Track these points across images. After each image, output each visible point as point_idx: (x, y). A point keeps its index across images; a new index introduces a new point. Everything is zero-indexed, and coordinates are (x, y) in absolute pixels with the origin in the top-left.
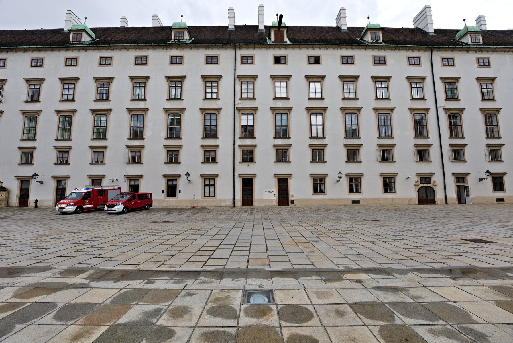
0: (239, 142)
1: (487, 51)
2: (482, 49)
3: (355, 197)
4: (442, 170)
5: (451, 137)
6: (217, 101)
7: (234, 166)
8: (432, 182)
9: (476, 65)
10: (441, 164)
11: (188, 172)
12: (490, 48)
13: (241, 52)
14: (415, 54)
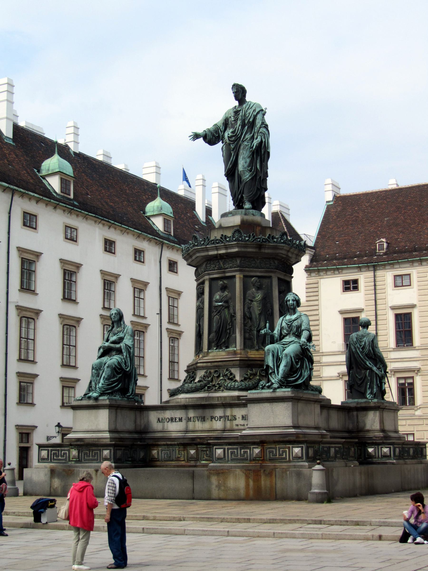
2: (72, 211)
5: (20, 360)
10: (3, 407)
12: (81, 212)
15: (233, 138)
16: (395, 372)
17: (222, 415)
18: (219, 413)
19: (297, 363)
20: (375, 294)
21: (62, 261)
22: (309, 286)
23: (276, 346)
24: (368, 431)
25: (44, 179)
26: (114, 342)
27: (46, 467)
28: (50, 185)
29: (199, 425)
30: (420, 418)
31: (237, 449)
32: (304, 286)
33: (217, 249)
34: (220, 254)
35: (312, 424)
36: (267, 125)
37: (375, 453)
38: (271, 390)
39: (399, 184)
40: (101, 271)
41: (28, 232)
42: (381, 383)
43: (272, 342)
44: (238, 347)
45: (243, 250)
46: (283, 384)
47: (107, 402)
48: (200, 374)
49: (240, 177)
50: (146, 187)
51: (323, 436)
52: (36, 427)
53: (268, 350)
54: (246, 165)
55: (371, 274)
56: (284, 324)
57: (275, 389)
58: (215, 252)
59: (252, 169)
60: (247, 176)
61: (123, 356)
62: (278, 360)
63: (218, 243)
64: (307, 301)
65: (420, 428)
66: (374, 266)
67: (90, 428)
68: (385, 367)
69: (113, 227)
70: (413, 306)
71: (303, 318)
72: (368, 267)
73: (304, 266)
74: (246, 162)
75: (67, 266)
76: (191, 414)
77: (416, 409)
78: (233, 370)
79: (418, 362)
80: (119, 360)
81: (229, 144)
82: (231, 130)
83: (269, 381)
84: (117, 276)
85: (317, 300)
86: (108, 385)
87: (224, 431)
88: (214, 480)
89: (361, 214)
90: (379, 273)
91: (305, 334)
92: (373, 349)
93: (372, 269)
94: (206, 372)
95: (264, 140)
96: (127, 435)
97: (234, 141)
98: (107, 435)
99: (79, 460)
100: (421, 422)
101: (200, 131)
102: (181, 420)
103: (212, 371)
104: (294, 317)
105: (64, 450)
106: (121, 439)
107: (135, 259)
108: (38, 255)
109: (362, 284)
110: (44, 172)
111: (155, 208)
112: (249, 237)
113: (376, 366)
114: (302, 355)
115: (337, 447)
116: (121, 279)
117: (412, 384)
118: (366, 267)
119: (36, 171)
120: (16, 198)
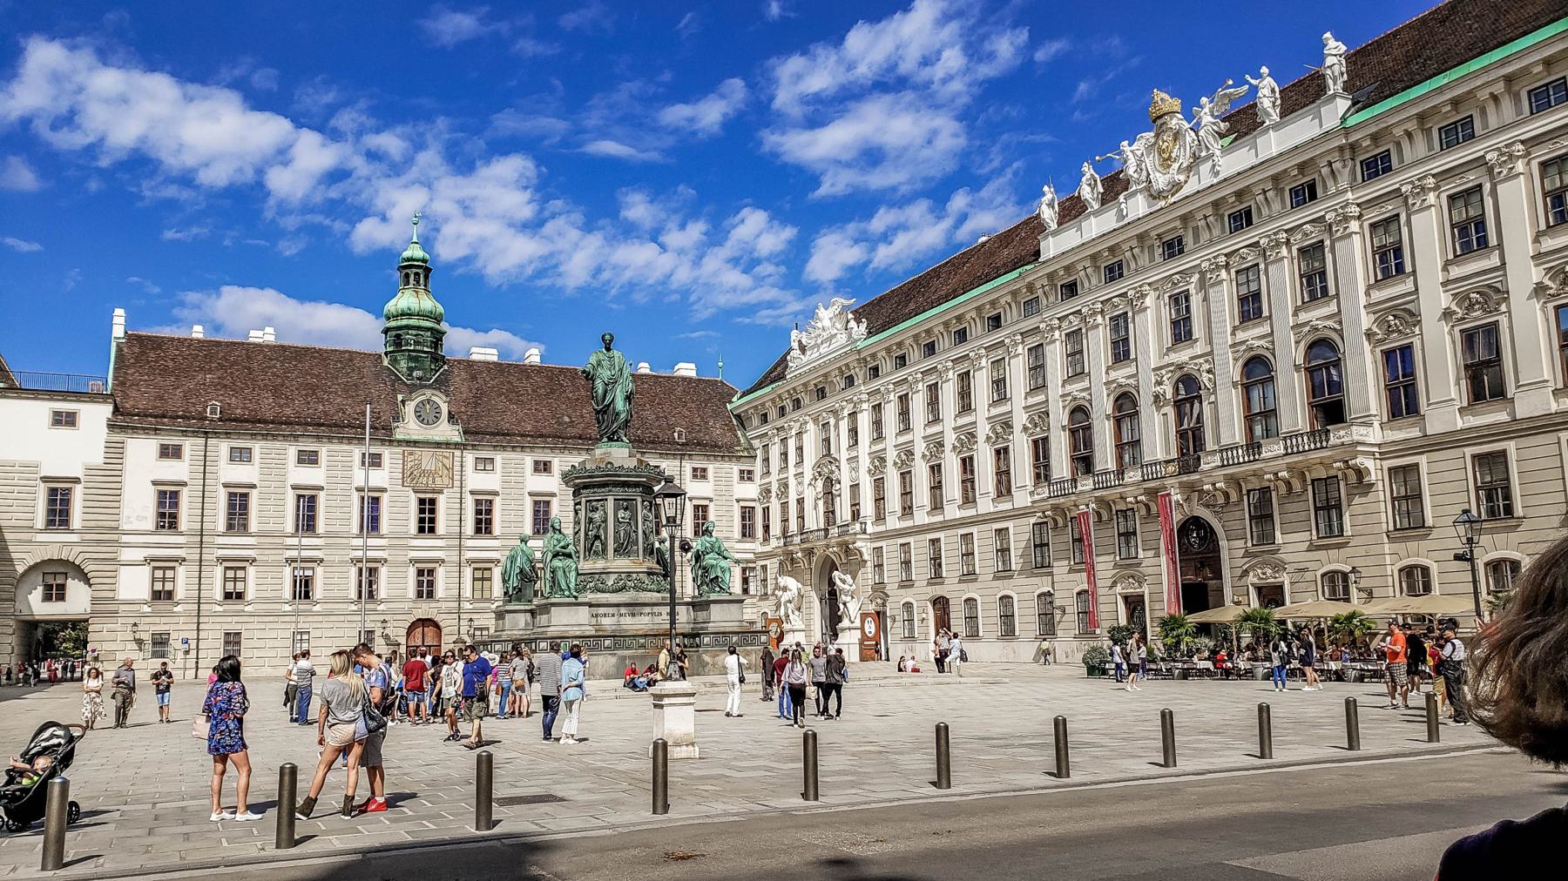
18: (647, 610)
22: (108, 445)
26: (563, 547)
29: (628, 620)
32: (103, 444)
33: (629, 476)
55: (202, 441)
56: (708, 545)
76: (623, 610)
89: (171, 364)
98: (591, 628)
100: (252, 619)
102: (613, 615)
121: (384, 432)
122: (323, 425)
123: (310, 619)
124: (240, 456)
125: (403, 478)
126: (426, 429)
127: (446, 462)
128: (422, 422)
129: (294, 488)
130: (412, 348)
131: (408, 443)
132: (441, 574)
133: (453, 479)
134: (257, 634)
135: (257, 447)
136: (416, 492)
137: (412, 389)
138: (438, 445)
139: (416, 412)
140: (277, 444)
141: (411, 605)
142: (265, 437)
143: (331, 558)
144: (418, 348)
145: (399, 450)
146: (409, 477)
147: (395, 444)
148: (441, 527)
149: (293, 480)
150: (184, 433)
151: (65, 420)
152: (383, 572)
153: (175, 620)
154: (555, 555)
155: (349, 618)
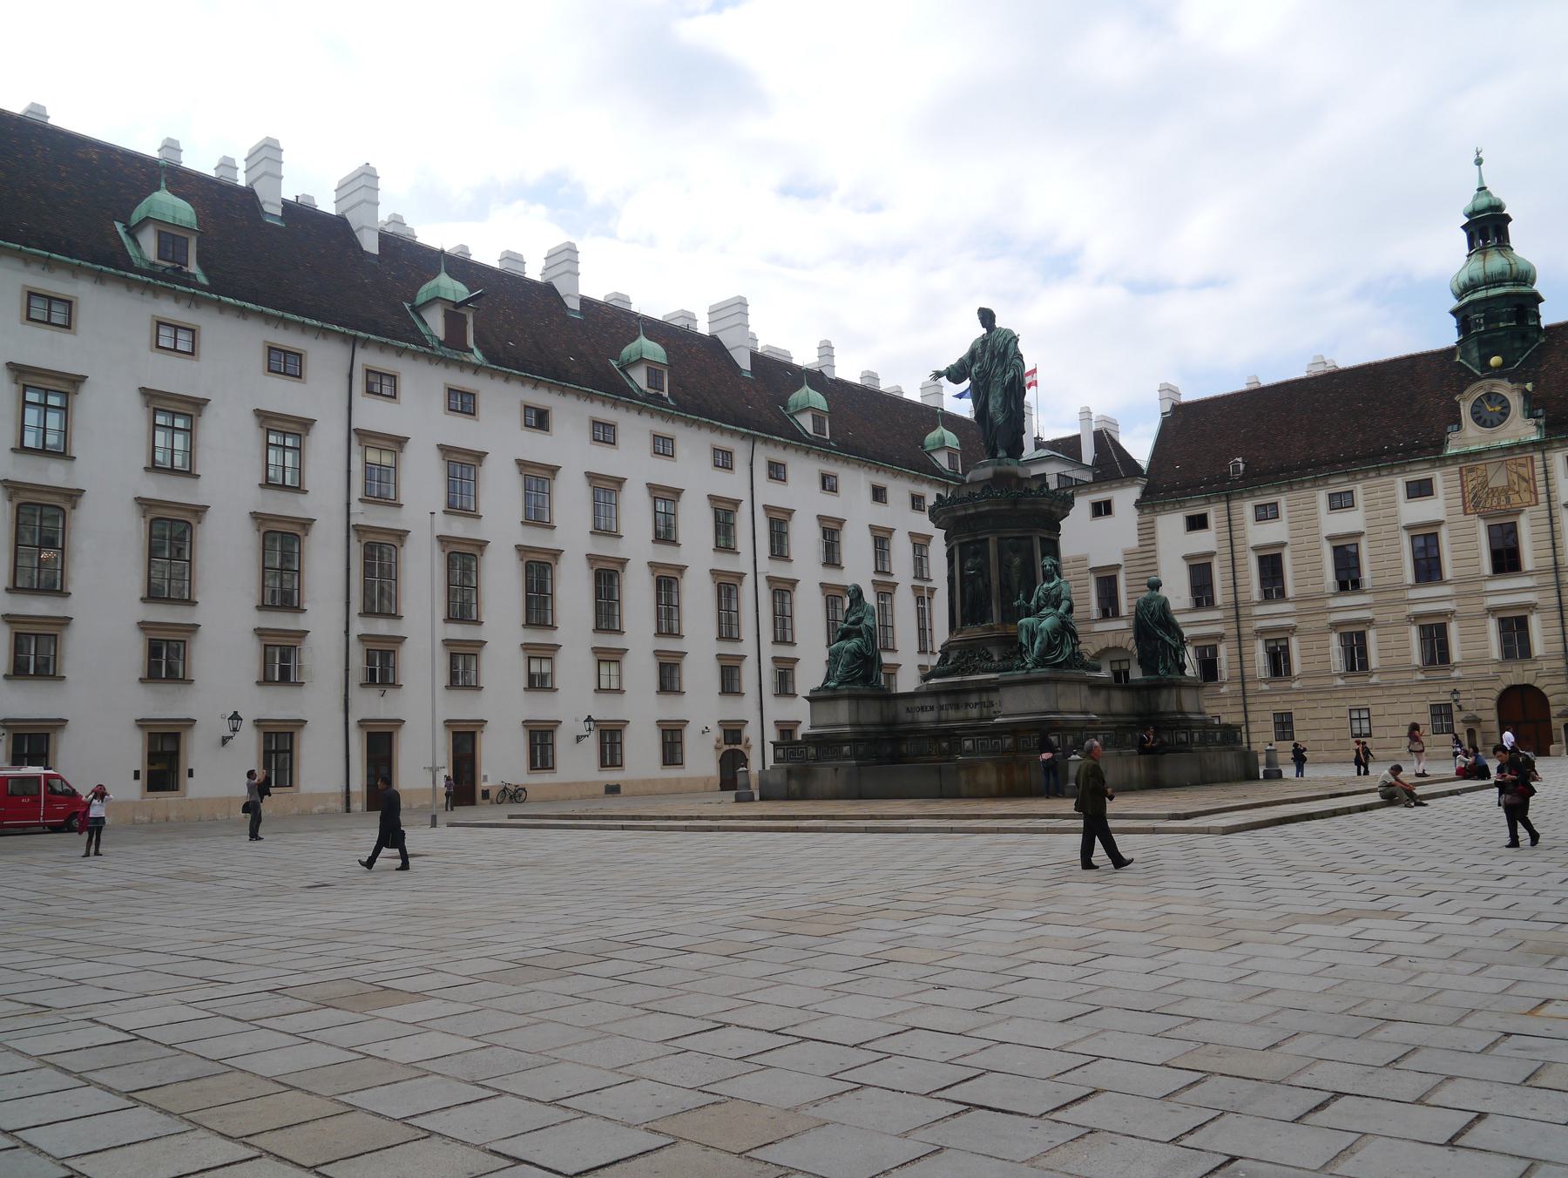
0: (359, 626)
1: (836, 460)
3: (612, 776)
4: (759, 713)
5: (775, 642)
6: (301, 497)
7: (346, 695)
8: (743, 741)
9: (818, 486)
10: (759, 700)
11: (236, 713)
13: (368, 358)
14: (725, 442)
15: (981, 375)
16: (1262, 633)
17: (977, 701)
18: (974, 699)
19: (1055, 638)
20: (1231, 531)
21: (820, 517)
23: (1031, 619)
24: (1162, 713)
25: (793, 417)
26: (853, 623)
27: (782, 768)
28: (799, 424)
29: (952, 714)
30: (1299, 692)
31: (987, 739)
32: (1136, 527)
34: (969, 514)
35: (1078, 708)
36: (1021, 355)
37: (1169, 740)
38: (1025, 671)
39: (1260, 382)
40: (870, 525)
41: (775, 486)
42: (1177, 656)
43: (1028, 615)
44: (995, 622)
45: (995, 508)
46: (1037, 664)
47: (846, 692)
48: (954, 654)
49: (991, 420)
50: (924, 414)
51: (1091, 721)
52: (800, 722)
53: (1021, 625)
54: (997, 406)
57: (1029, 669)
58: (963, 513)
59: (1004, 410)
60: (1000, 419)
61: (863, 638)
62: (1032, 636)
63: (966, 502)
64: (1140, 546)
65: (1299, 705)
66: (1227, 495)
67: (829, 722)
68: (1181, 635)
69: (883, 470)
70: (1283, 545)
71: (1063, 585)
72: (1220, 496)
73: (1134, 501)
74: (997, 402)
75: (827, 523)
76: (943, 702)
77: (1293, 680)
78: (989, 649)
79: (1293, 619)
80: (859, 643)
81: (977, 382)
82: (978, 365)
83: (1024, 660)
84: (891, 531)
85: (1154, 544)
86: (848, 672)
87: (981, 719)
88: (963, 775)
90: (1233, 504)
91: (1065, 605)
92: (1165, 616)
93: (1224, 499)
94: (960, 653)
95: (1017, 373)
96: (872, 729)
97: (983, 378)
99: (817, 759)
100: (1301, 697)
101: (942, 368)
102: (932, 708)
103: (967, 651)
104: (1052, 585)
105: (801, 748)
106: (864, 733)
107: (913, 508)
108: (790, 512)
109: (1212, 520)
110: (792, 410)
111: (936, 440)
112: (1002, 493)
113: (1169, 636)
114: (1062, 628)
115: (1107, 734)
116: (895, 534)
117: (1286, 649)
118: (1216, 496)
119: (781, 408)
120: (758, 446)
121: (1431, 449)
122: (1356, 458)
123: (1367, 693)
124: (1267, 513)
125: (1464, 504)
126: (1493, 433)
127: (1523, 471)
128: (1484, 425)
129: (1330, 538)
130: (1483, 329)
131: (1468, 456)
132: (1535, 623)
133: (1536, 493)
134: (1311, 714)
135: (1283, 501)
136: (1485, 518)
137: (1479, 379)
138: (1510, 449)
139: (1473, 413)
140: (1305, 493)
141: (1496, 668)
142: (1290, 487)
143: (1385, 617)
144: (1492, 326)
145: (1456, 469)
146: (1473, 503)
147: (1449, 462)
148: (1528, 560)
149: (1326, 533)
150: (1208, 501)
151: (1102, 509)
152: (1453, 630)
153: (1222, 702)
154: (846, 635)
155: (1416, 690)
